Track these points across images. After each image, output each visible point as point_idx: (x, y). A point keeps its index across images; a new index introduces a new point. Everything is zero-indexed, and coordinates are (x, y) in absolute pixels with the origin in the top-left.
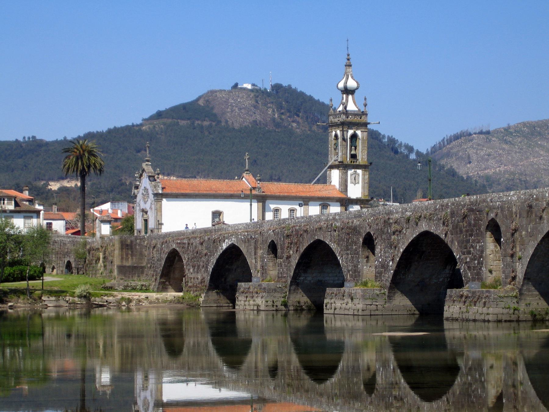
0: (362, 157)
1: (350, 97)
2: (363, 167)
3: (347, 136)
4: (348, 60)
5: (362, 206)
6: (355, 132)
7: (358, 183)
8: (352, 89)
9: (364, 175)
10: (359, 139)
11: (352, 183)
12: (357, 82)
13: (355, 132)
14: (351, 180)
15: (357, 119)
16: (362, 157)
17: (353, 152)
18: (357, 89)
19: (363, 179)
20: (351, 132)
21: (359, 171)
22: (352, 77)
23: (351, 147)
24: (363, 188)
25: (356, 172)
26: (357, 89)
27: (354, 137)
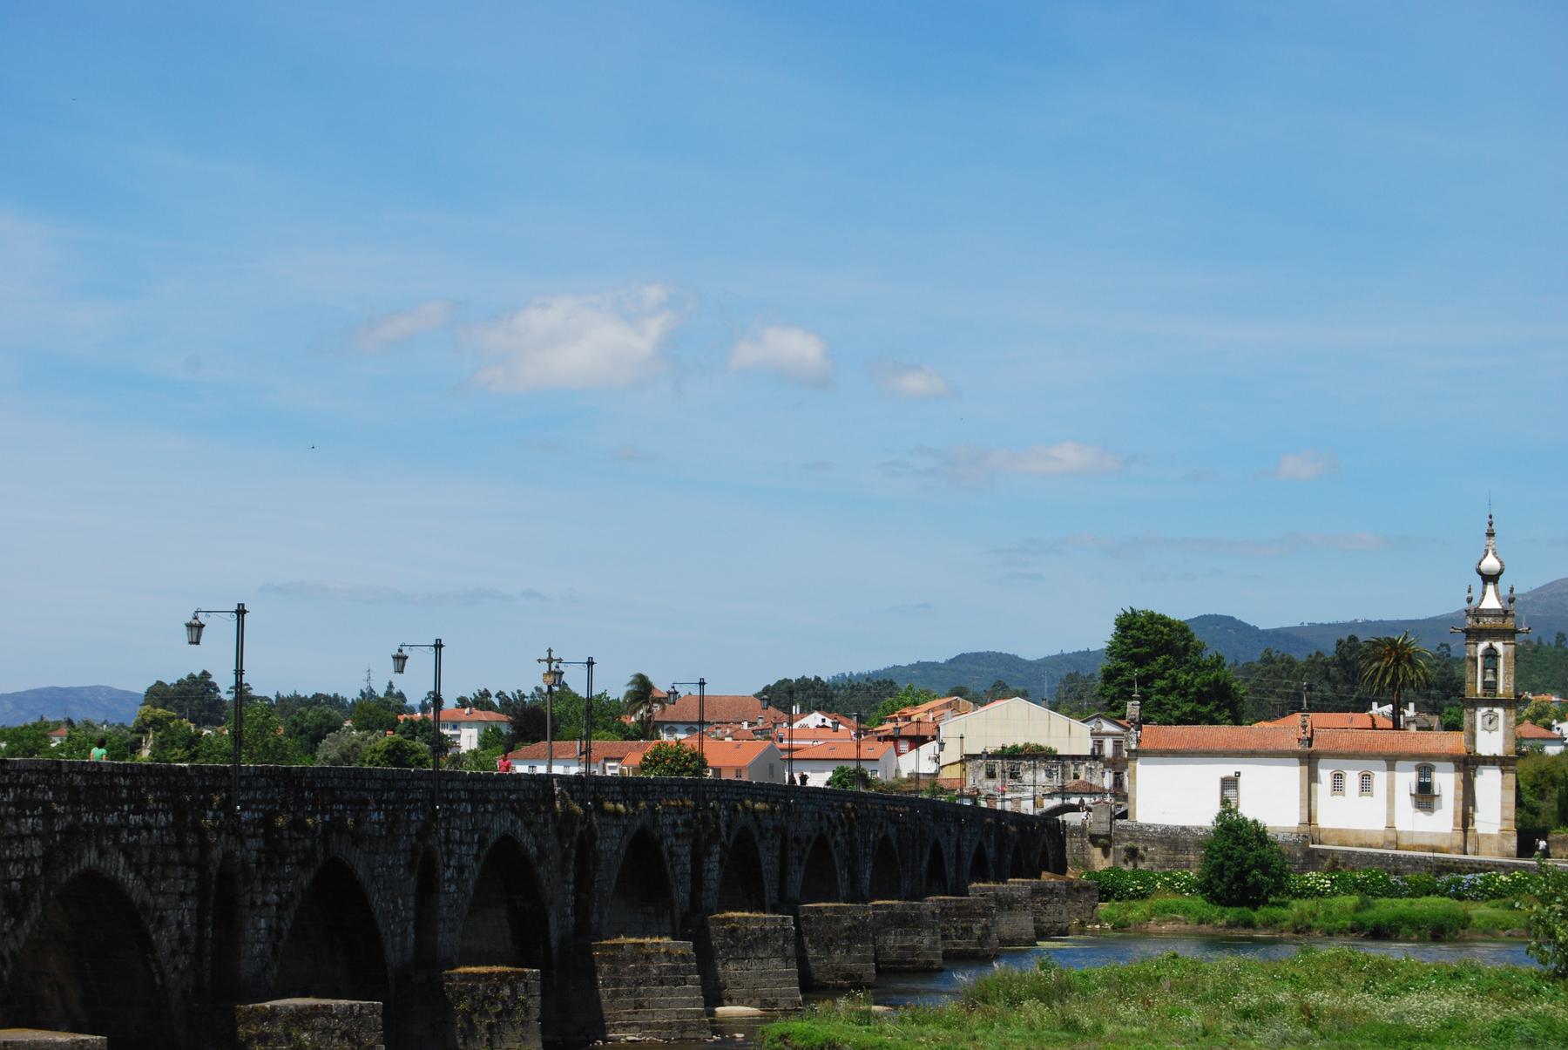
0: (1504, 686)
1: (1490, 588)
2: (1506, 704)
3: (1476, 653)
4: (1491, 525)
5: (1503, 768)
6: (1491, 645)
7: (1496, 729)
8: (1494, 574)
9: (1506, 716)
10: (1500, 656)
11: (1484, 729)
12: (1501, 562)
13: (1491, 645)
14: (1483, 723)
15: (1498, 623)
16: (1504, 686)
17: (1490, 678)
18: (1501, 572)
19: (1506, 723)
20: (1483, 645)
21: (1499, 711)
22: (1495, 554)
23: (1484, 669)
24: (1506, 737)
25: (1492, 711)
26: (1501, 572)
27: (1491, 655)
